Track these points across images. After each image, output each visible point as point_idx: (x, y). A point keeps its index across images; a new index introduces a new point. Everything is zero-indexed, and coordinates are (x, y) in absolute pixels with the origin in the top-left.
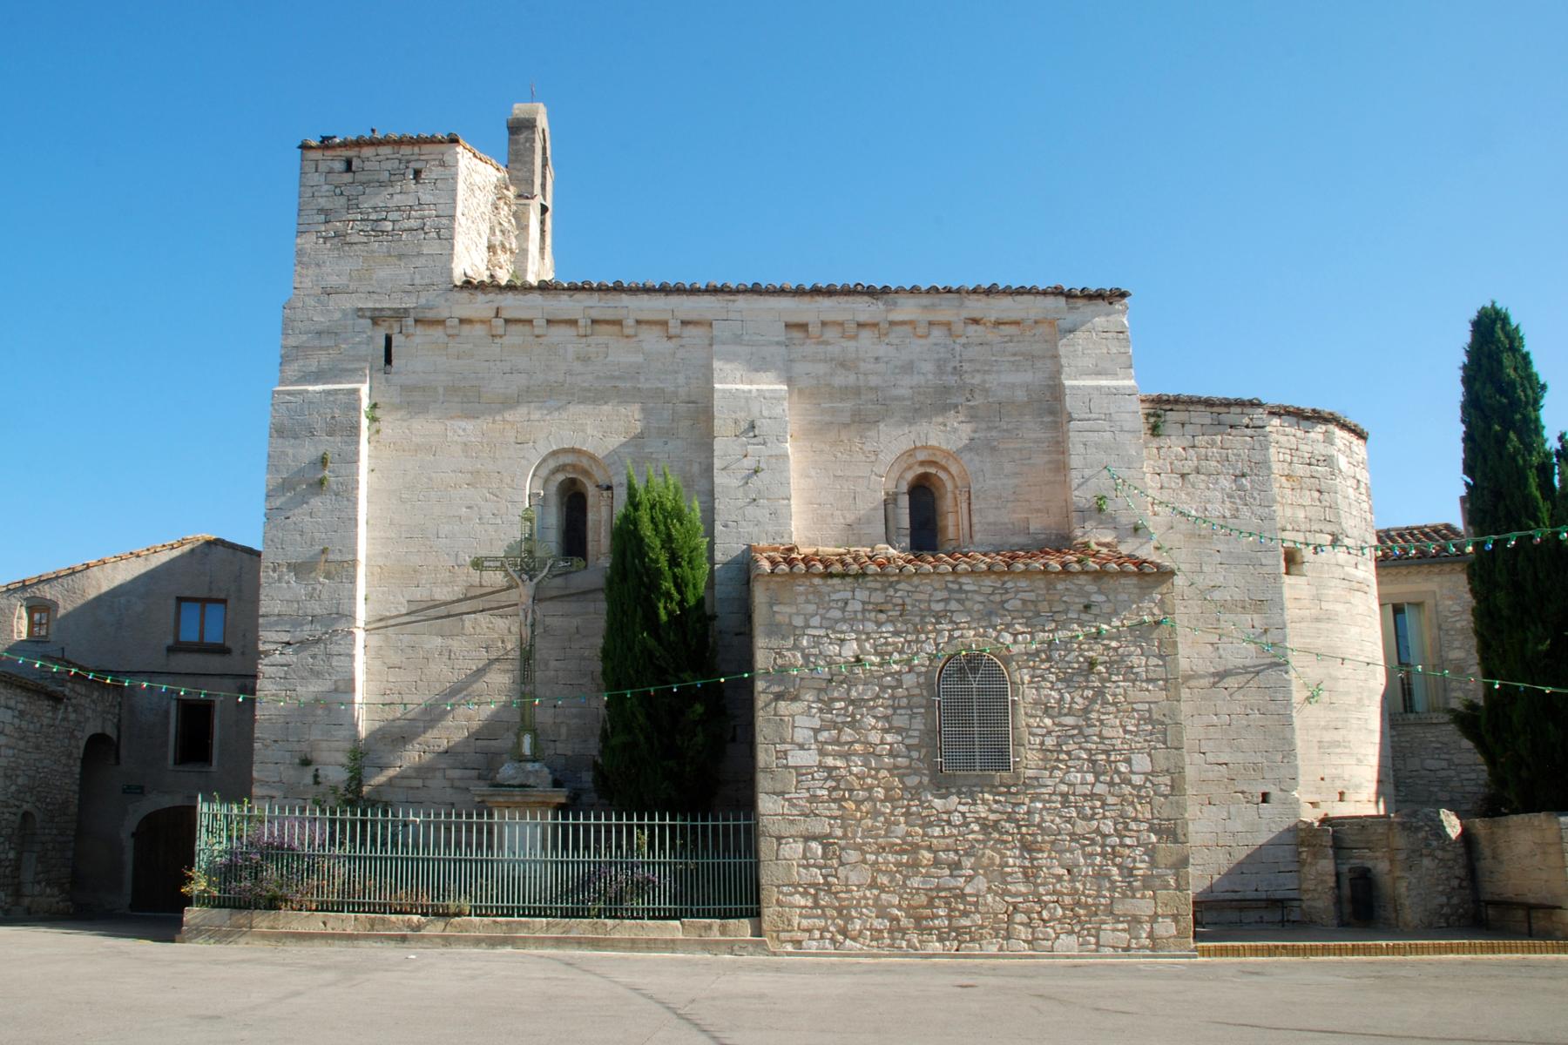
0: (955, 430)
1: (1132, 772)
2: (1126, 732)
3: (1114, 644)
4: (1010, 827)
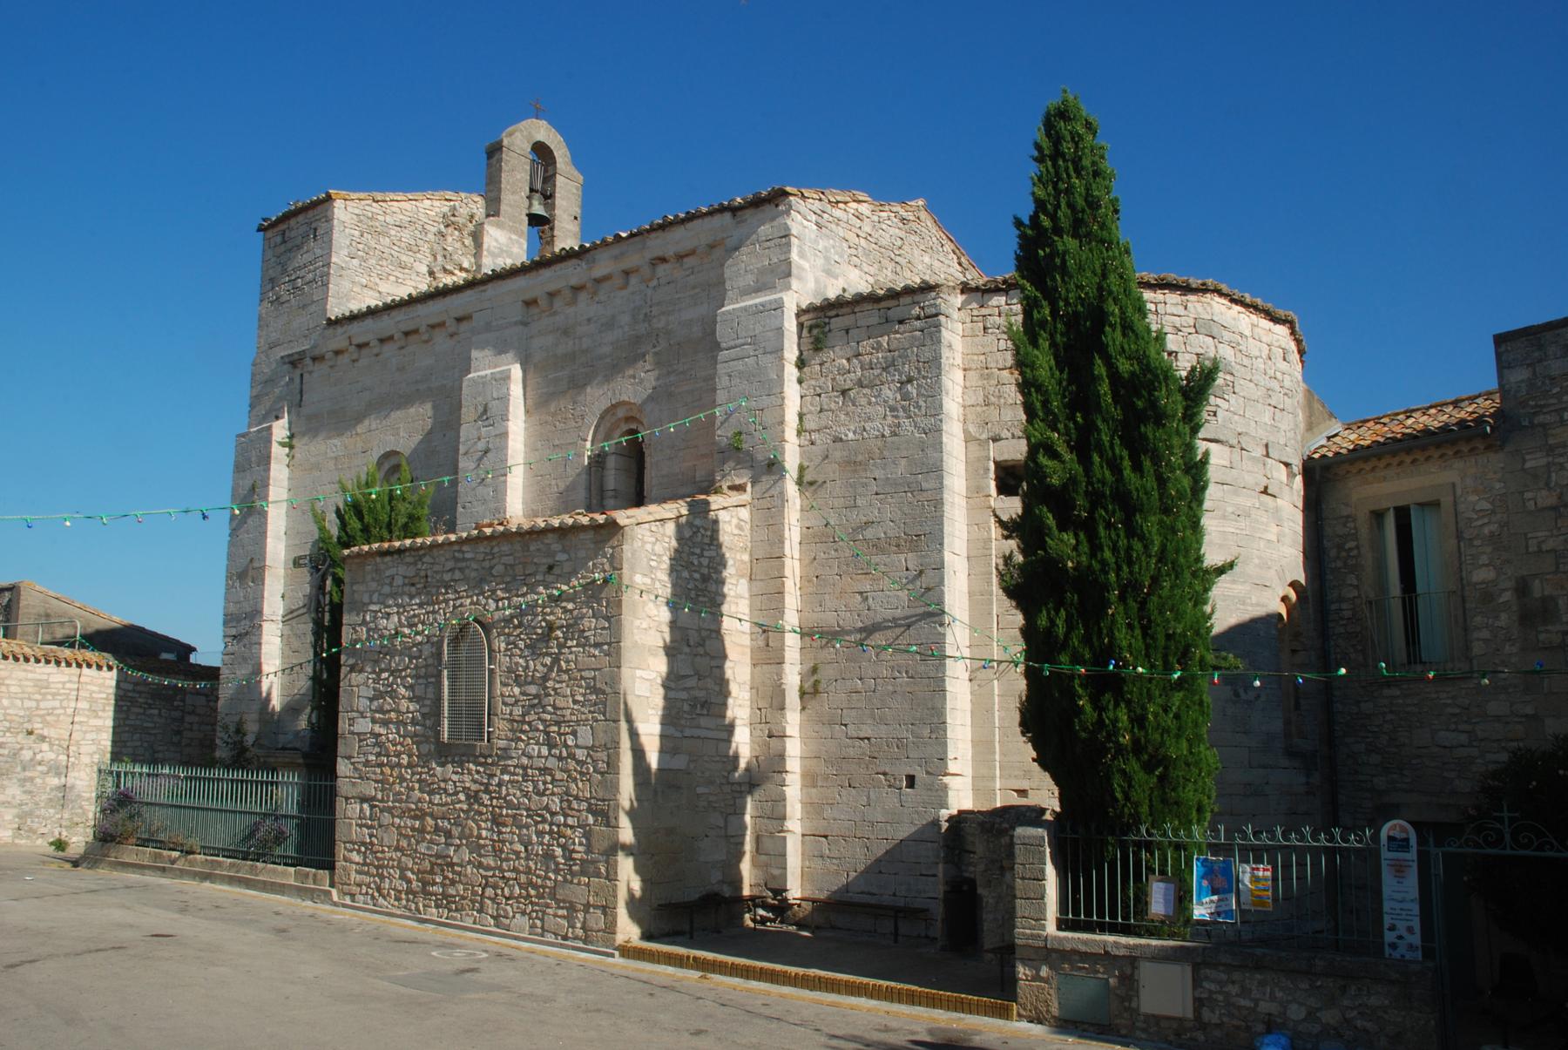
0: (642, 381)
1: (577, 746)
2: (575, 702)
3: (570, 606)
4: (485, 797)
